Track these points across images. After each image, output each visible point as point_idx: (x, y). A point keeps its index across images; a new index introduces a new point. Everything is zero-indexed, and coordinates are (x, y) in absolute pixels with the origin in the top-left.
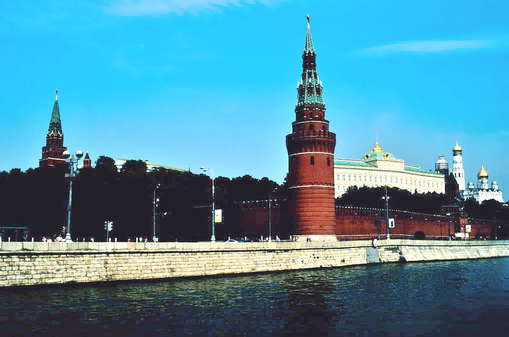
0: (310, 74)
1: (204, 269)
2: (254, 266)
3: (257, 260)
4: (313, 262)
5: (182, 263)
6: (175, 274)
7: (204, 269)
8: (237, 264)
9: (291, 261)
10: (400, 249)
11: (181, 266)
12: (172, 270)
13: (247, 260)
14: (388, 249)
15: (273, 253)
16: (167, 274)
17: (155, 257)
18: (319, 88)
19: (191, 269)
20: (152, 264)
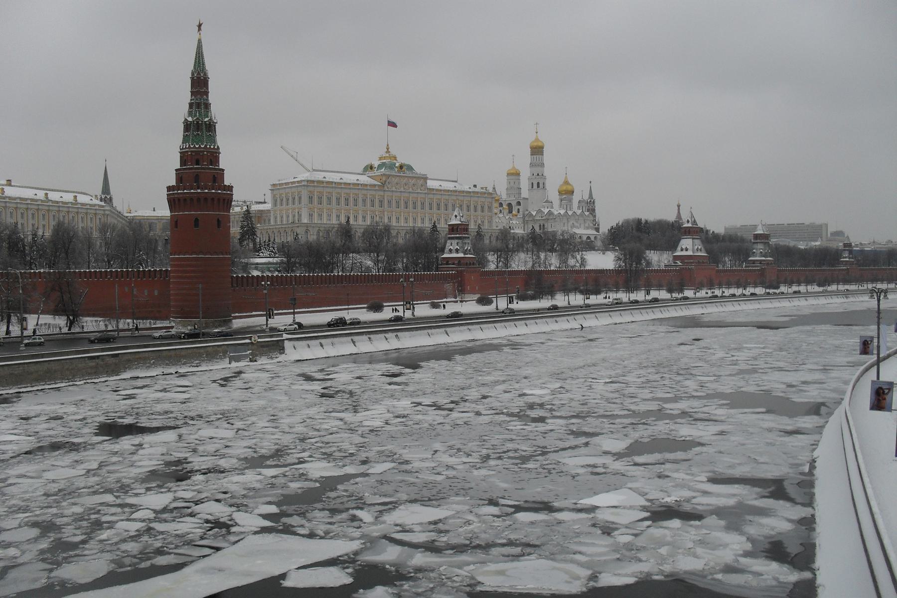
15: (97, 361)
18: (210, 124)
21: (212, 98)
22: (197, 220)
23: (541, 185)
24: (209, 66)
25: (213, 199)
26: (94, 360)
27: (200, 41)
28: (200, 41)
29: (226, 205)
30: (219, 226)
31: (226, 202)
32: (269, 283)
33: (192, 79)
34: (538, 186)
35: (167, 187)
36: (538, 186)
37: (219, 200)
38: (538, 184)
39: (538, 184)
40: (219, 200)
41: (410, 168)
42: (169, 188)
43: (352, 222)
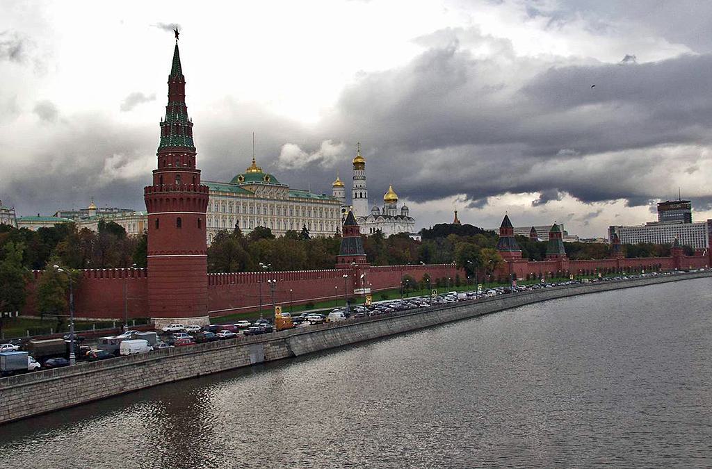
0: (177, 108)
1: (66, 398)
2: (122, 385)
3: (126, 378)
4: (189, 370)
5: (42, 396)
6: (34, 411)
7: (66, 398)
8: (104, 386)
9: (163, 372)
10: (288, 342)
11: (42, 400)
12: (32, 406)
13: (114, 380)
14: (274, 344)
16: (25, 413)
17: (13, 394)
19: (52, 401)
20: (9, 403)
21: (188, 101)
22: (179, 220)
23: (363, 196)
24: (185, 71)
25: (195, 199)
26: (141, 367)
27: (177, 47)
28: (177, 47)
29: (201, 205)
30: (199, 227)
31: (197, 201)
32: (275, 281)
33: (170, 83)
34: (361, 197)
35: (146, 188)
36: (361, 197)
37: (200, 200)
38: (361, 194)
39: (361, 194)
40: (200, 200)
41: (273, 179)
42: (147, 189)
43: (241, 226)
